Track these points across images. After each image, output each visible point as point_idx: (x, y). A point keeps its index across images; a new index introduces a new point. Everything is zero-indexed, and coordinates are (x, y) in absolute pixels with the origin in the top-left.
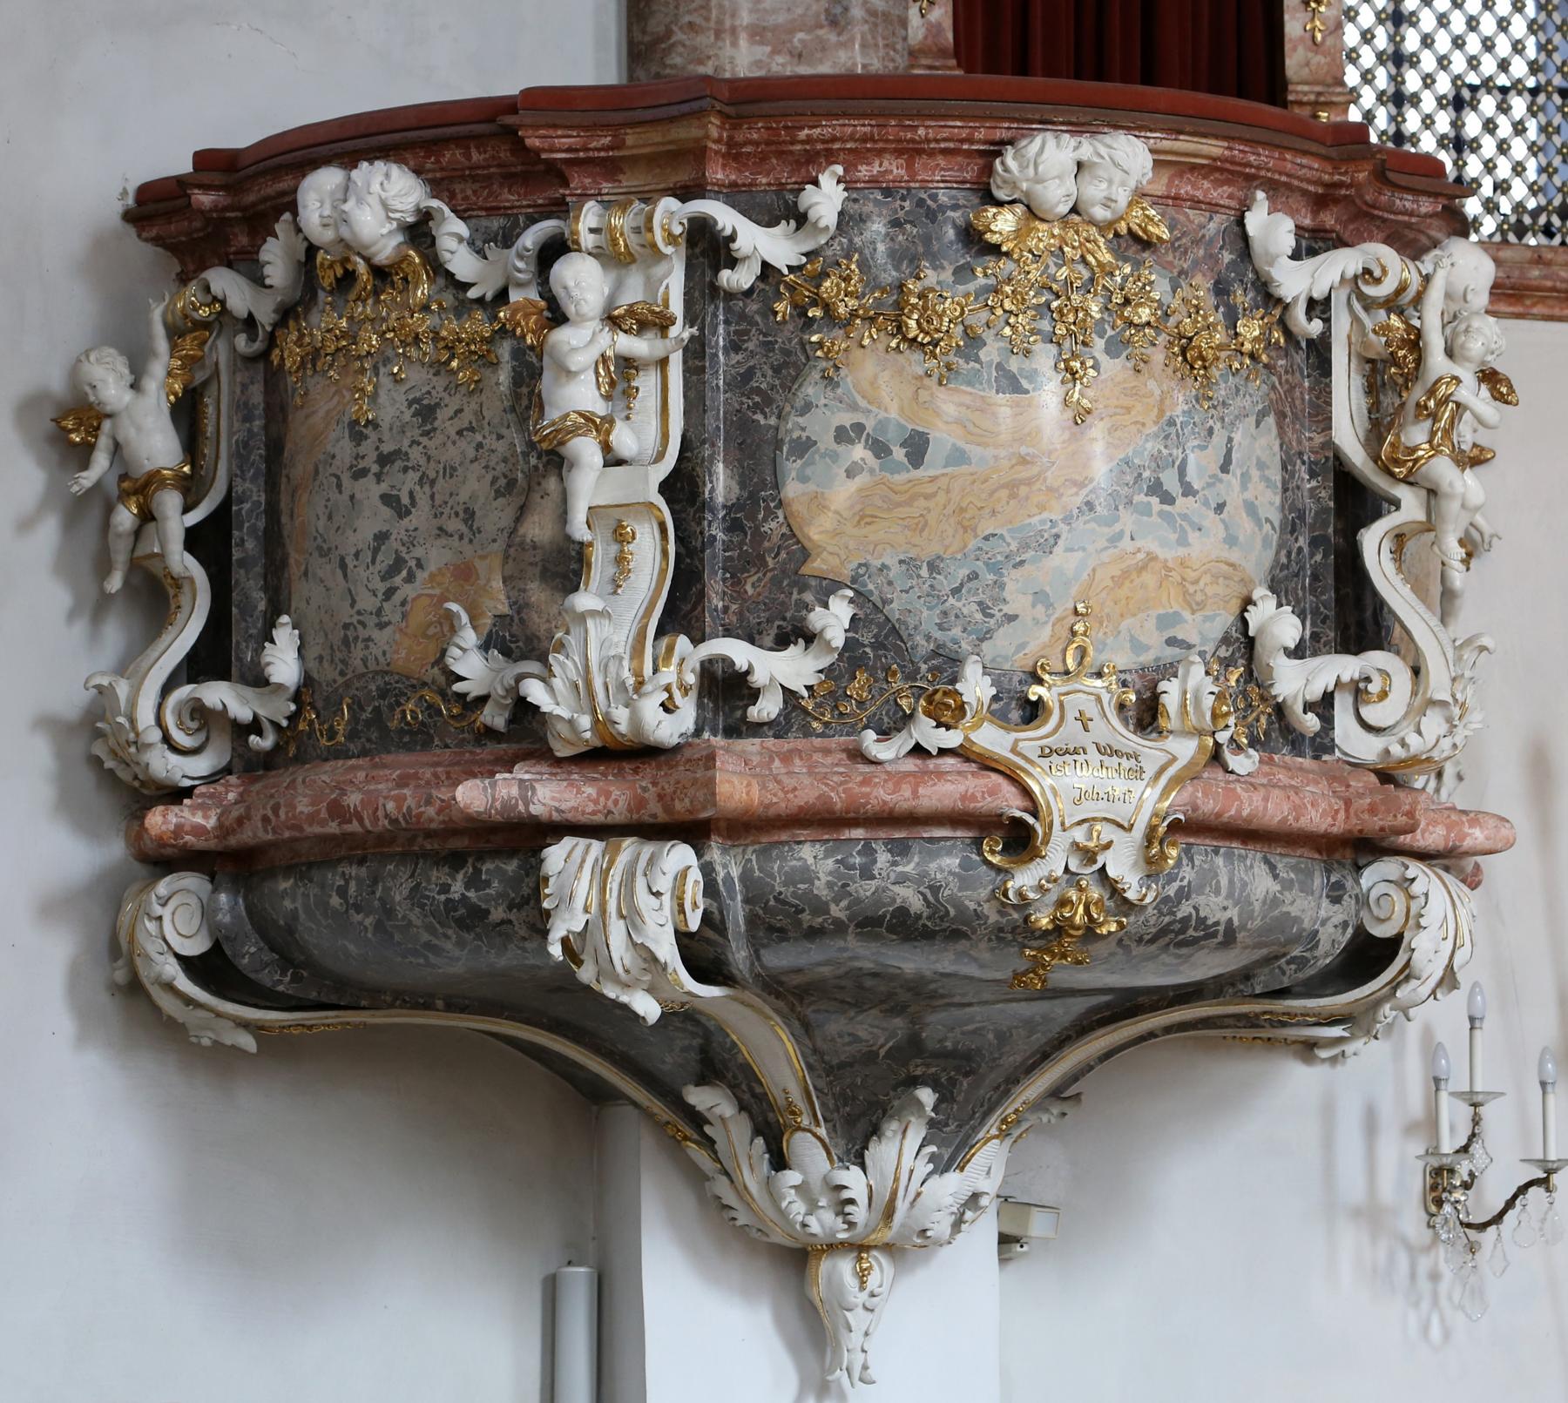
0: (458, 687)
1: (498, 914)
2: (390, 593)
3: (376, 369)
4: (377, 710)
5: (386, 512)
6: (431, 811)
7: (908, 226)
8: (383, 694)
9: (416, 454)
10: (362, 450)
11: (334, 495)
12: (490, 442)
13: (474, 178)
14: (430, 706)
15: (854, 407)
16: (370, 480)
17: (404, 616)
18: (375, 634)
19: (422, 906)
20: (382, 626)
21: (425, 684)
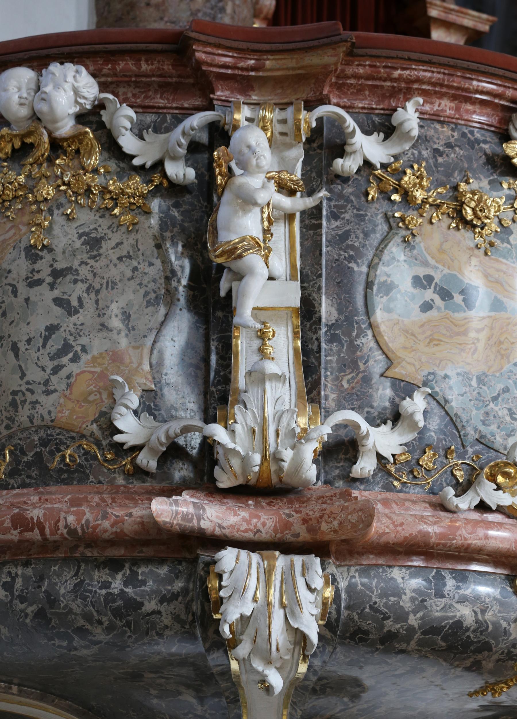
0: (118, 438)
1: (150, 606)
2: (56, 370)
3: (50, 211)
4: (38, 455)
5: (58, 310)
6: (106, 524)
7: (457, 149)
8: (44, 443)
9: (84, 271)
10: (37, 267)
11: (9, 299)
12: (143, 267)
13: (137, 85)
14: (86, 453)
15: (426, 264)
16: (44, 289)
17: (69, 386)
18: (43, 399)
19: (84, 598)
20: (48, 393)
21: (83, 436)
